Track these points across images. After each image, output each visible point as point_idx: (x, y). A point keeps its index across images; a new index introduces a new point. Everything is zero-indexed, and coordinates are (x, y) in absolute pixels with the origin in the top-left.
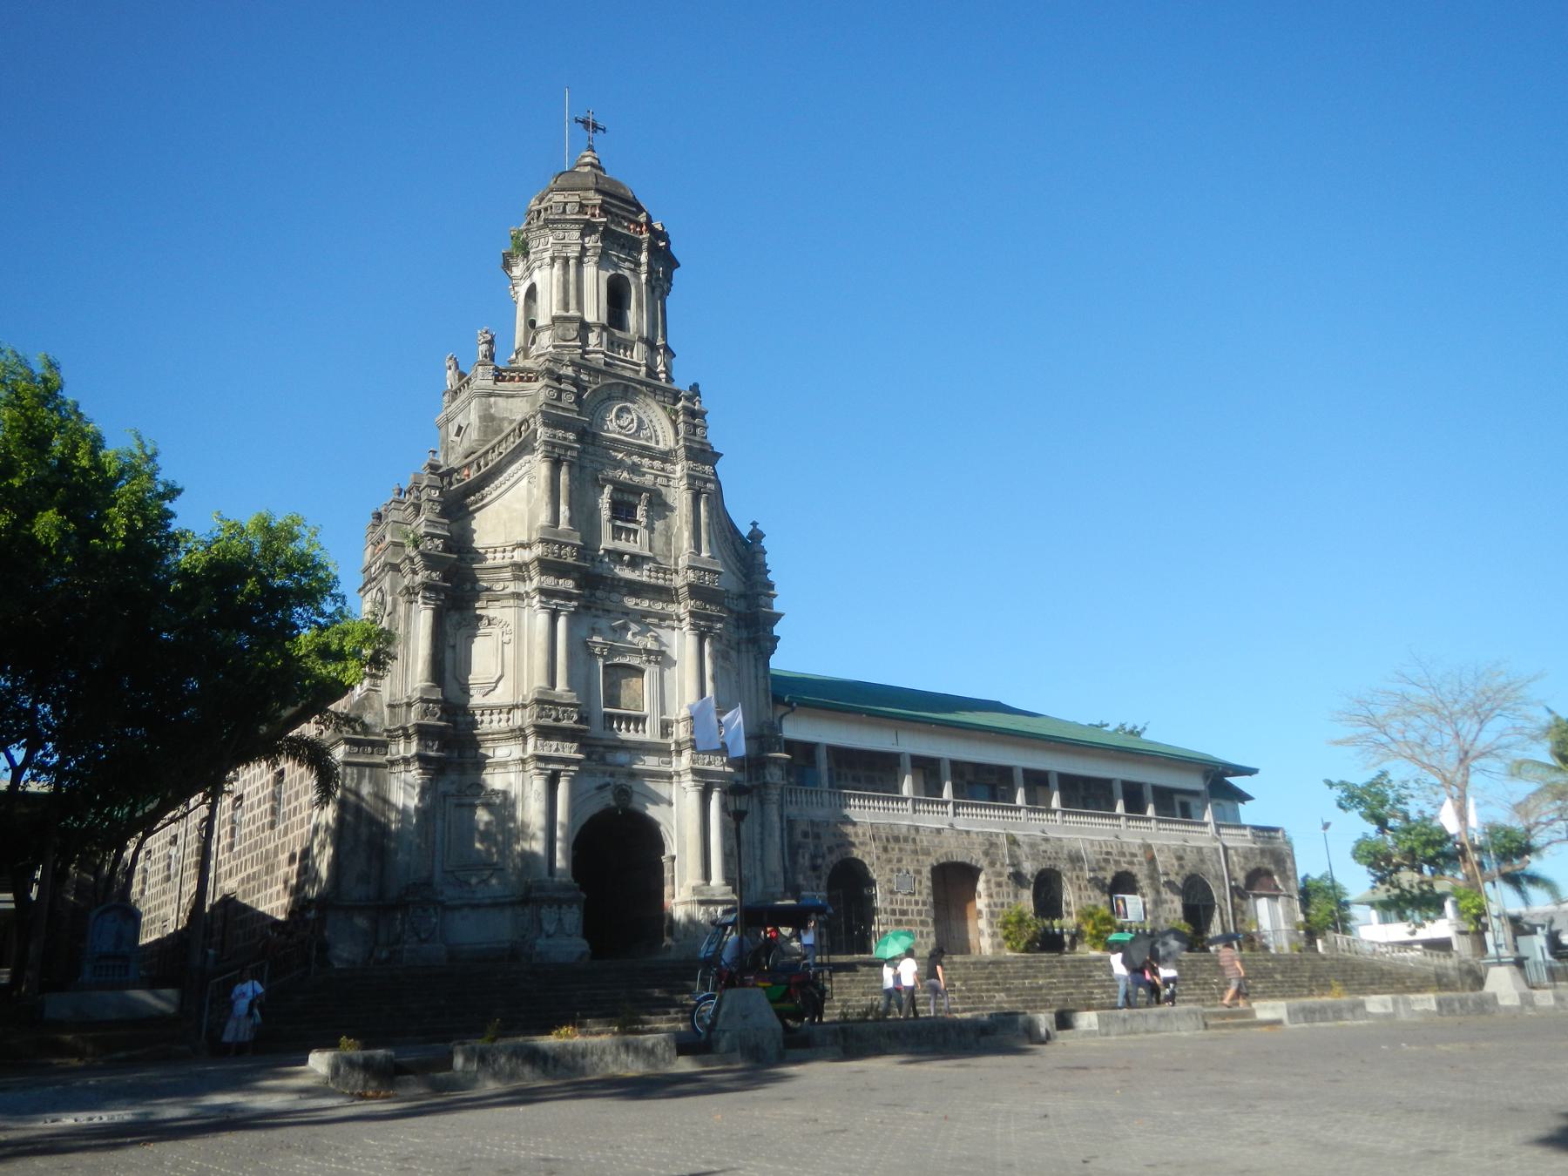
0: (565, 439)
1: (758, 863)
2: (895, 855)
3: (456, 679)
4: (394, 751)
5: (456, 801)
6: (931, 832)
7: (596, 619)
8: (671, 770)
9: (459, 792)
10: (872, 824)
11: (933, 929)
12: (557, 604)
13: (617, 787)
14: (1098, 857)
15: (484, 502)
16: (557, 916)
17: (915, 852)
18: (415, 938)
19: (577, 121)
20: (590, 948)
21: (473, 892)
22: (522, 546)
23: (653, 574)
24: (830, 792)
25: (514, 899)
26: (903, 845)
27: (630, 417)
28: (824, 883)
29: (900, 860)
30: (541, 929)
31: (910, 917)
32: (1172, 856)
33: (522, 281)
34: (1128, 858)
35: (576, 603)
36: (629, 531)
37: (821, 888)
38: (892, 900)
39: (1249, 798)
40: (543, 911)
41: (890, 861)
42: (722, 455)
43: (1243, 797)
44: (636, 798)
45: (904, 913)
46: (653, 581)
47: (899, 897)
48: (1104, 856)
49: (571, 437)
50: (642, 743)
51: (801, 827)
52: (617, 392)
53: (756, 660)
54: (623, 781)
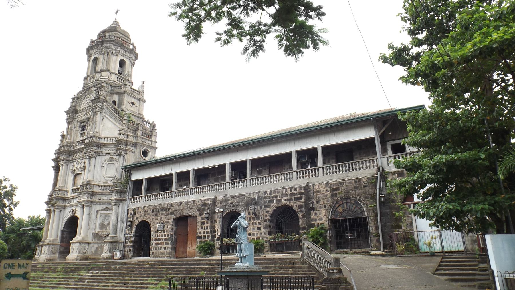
6: (177, 204)
10: (154, 206)
11: (170, 246)
12: (62, 163)
17: (168, 214)
26: (165, 212)
29: (161, 219)
31: (161, 242)
32: (329, 189)
34: (289, 197)
35: (64, 161)
37: (132, 233)
38: (156, 235)
41: (157, 219)
45: (159, 240)
47: (158, 233)
48: (271, 199)
54: (74, 208)
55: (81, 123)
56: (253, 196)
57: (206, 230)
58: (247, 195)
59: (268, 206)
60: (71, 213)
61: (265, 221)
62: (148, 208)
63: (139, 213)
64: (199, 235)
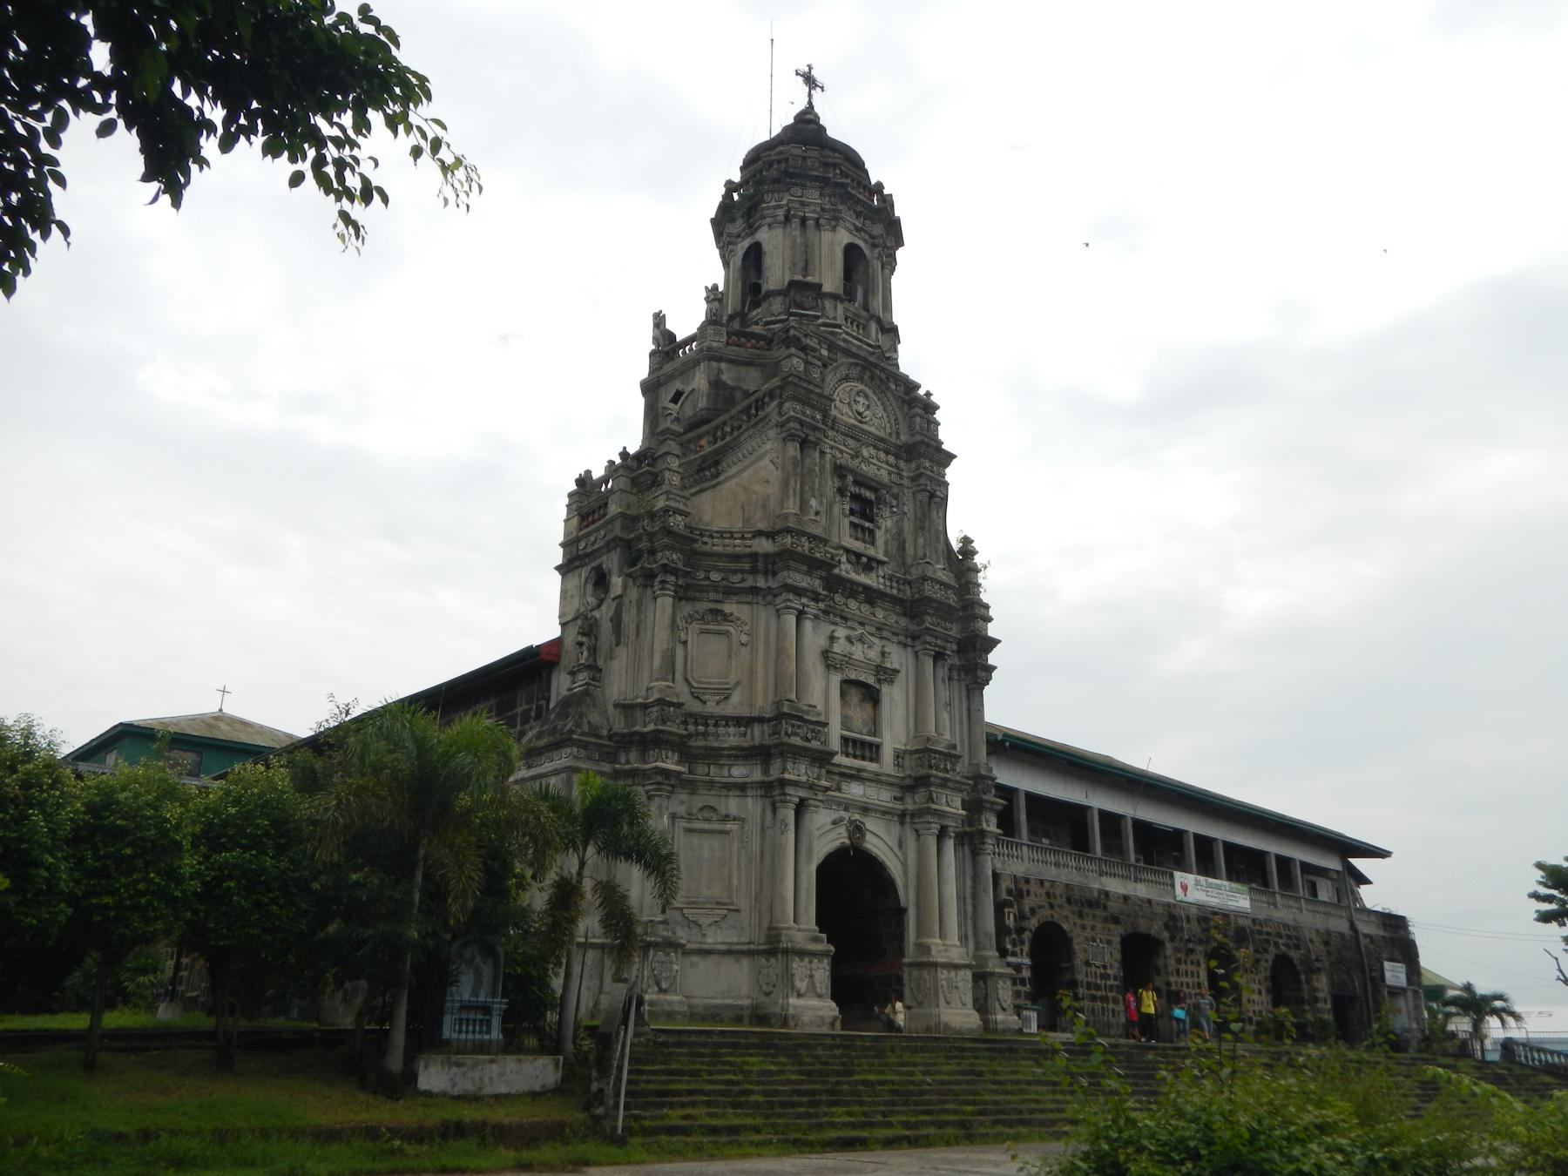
0: (813, 418)
1: (970, 922)
2: (1088, 922)
3: (687, 680)
4: (623, 759)
5: (686, 825)
7: (833, 627)
8: (901, 807)
9: (689, 814)
10: (1067, 885)
12: (804, 605)
13: (851, 822)
14: (1261, 937)
15: (722, 478)
16: (809, 972)
18: (656, 989)
19: (797, 74)
20: (840, 1013)
21: (704, 935)
22: (759, 534)
23: (888, 583)
24: (1028, 846)
25: (752, 947)
26: (1097, 912)
27: (867, 403)
28: (1026, 948)
29: (1093, 928)
30: (793, 987)
33: (740, 240)
36: (863, 529)
37: (1024, 954)
39: (1367, 882)
40: (795, 965)
42: (955, 457)
43: (1362, 880)
44: (869, 837)
46: (888, 590)
47: (1093, 969)
48: (1266, 937)
49: (818, 417)
50: (877, 774)
51: (1006, 884)
52: (854, 372)
53: (968, 690)
54: (857, 817)
55: (856, 483)
56: (1242, 922)
57: (1185, 980)
58: (1232, 917)
59: (1266, 951)
60: (842, 831)
61: (1266, 978)
62: (1052, 886)
63: (1032, 896)
64: (1174, 988)
